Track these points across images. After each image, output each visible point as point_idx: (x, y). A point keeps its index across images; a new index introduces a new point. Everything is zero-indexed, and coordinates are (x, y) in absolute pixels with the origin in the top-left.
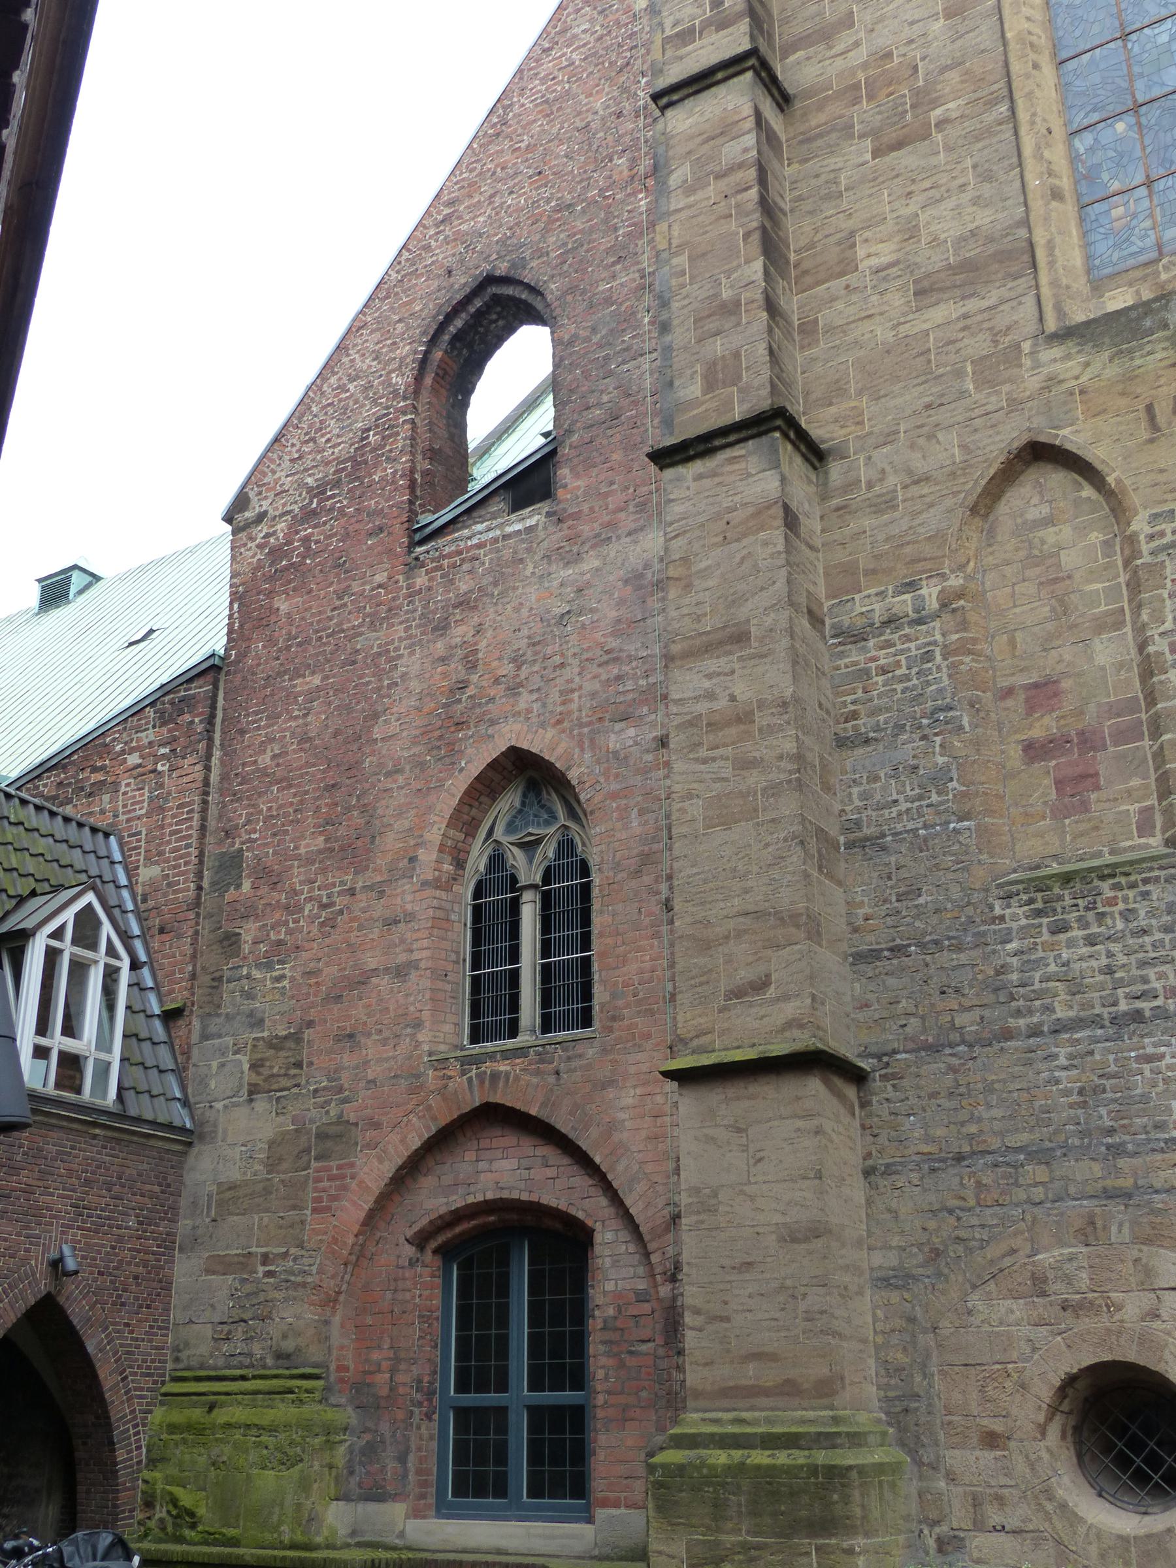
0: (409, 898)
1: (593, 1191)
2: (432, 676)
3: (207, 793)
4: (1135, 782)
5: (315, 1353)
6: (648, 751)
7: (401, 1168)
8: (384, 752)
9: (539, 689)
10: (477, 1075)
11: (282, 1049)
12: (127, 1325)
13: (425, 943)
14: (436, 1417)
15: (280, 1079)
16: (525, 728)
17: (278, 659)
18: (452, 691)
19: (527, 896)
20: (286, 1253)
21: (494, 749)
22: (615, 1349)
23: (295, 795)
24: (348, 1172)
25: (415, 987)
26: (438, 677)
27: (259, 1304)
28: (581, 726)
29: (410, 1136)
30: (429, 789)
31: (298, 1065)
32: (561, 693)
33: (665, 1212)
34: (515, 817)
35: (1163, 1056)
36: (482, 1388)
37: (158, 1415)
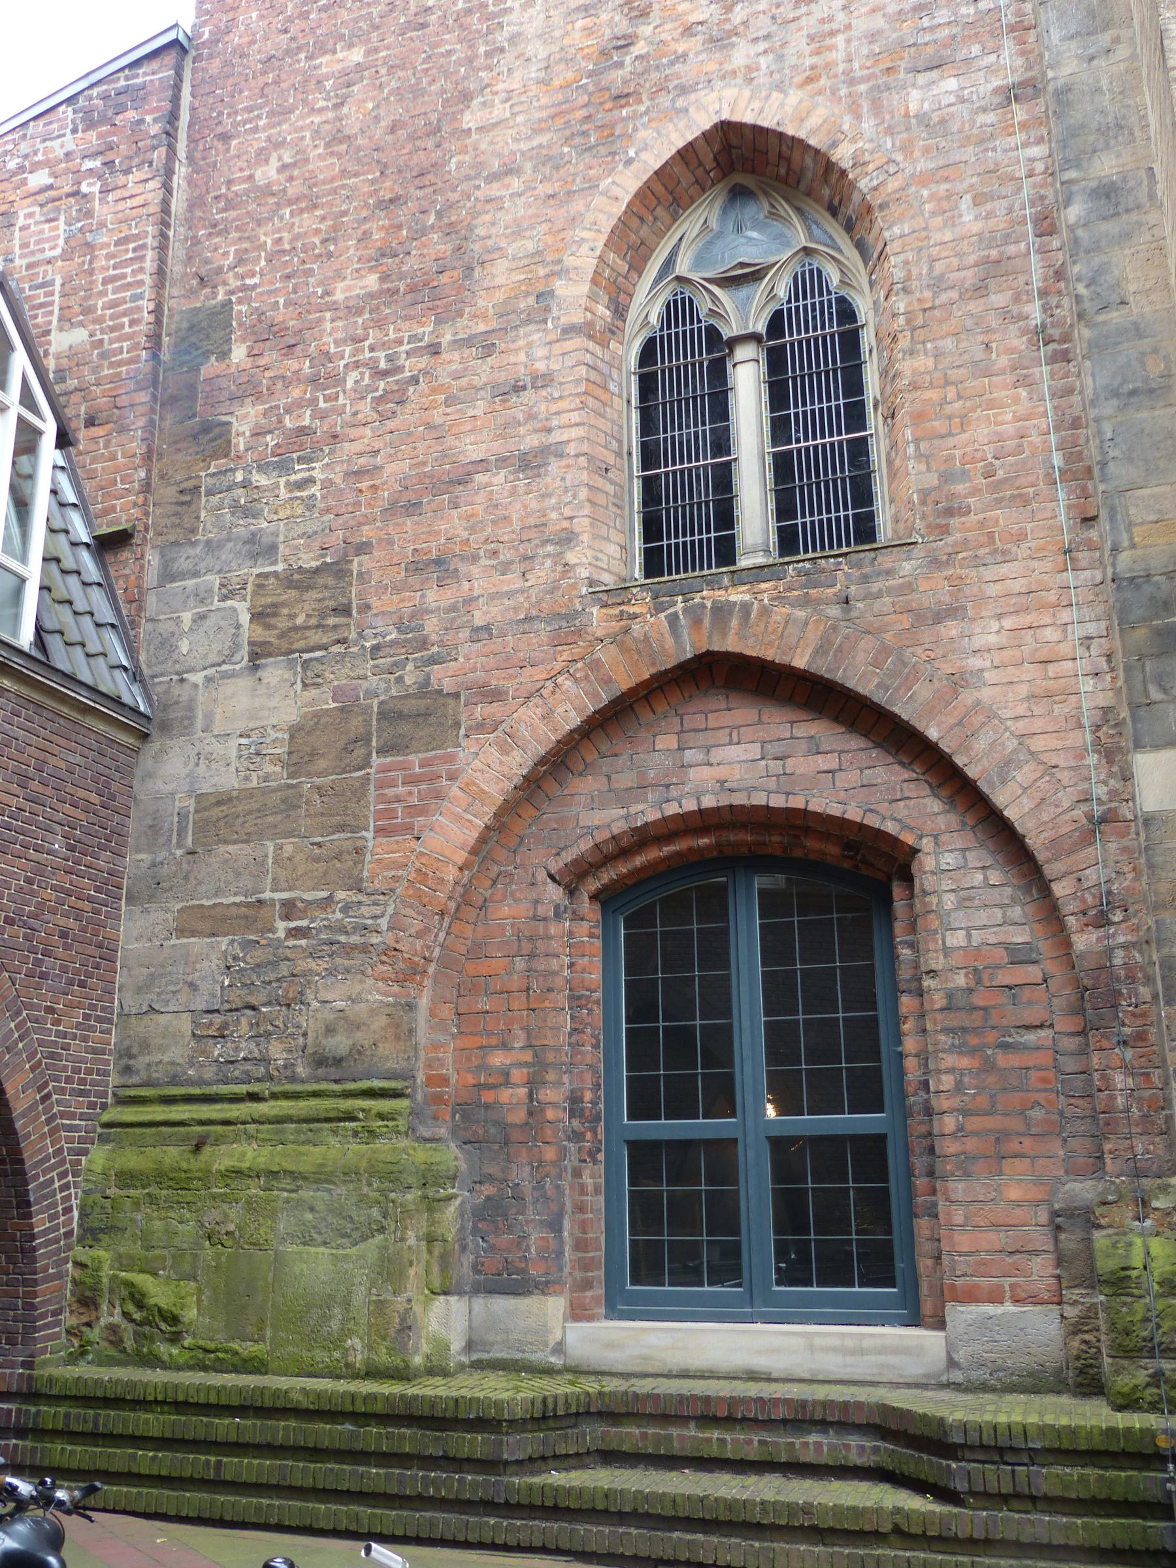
0: (541, 352)
1: (911, 789)
2: (567, 33)
3: (165, 224)
5: (389, 1055)
6: (985, 110)
7: (542, 761)
8: (483, 146)
9: (767, 37)
10: (685, 610)
11: (309, 587)
12: (50, 1010)
13: (575, 417)
14: (601, 1156)
15: (308, 633)
16: (747, 93)
17: (286, 31)
18: (604, 53)
19: (744, 352)
20: (329, 900)
21: (689, 127)
22: (974, 1041)
23: (323, 218)
24: (443, 769)
25: (558, 483)
26: (577, 35)
27: (278, 980)
28: (852, 82)
29: (560, 710)
30: (569, 193)
31: (345, 611)
32: (811, 38)
33: (1078, 813)
34: (710, 243)
36: (681, 1108)
37: (98, 1157)
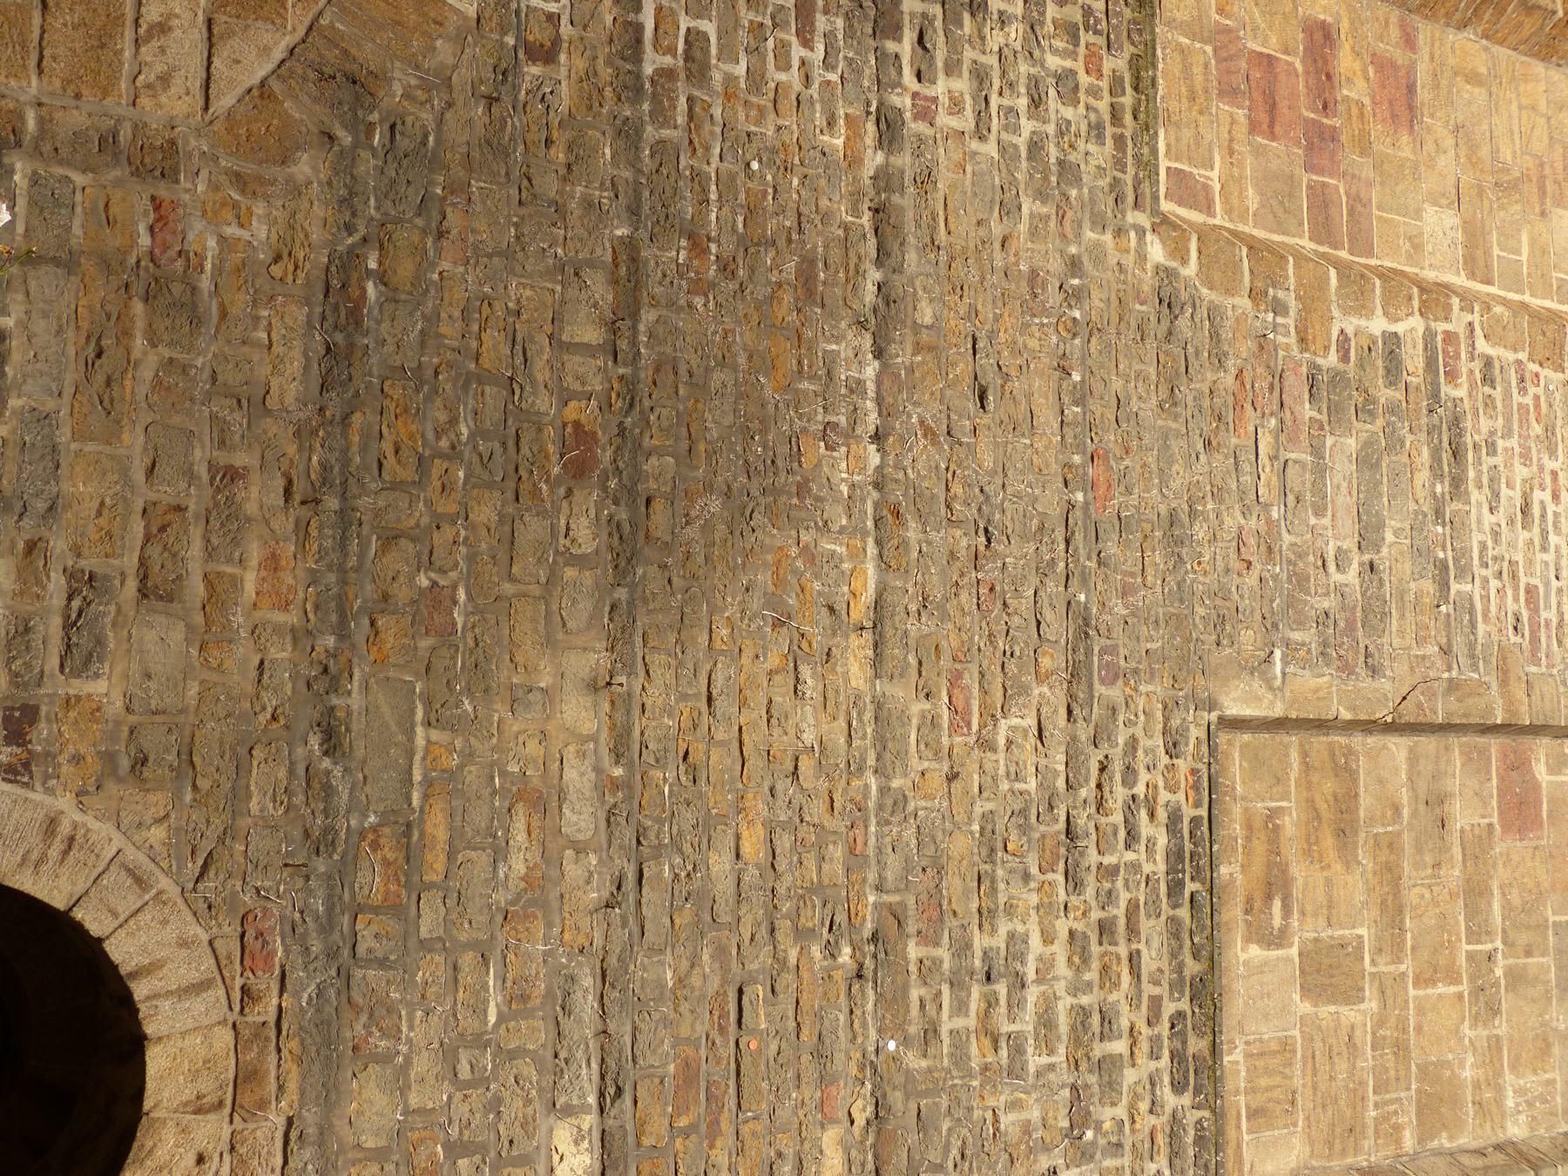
4: (1252, 200)
35: (807, 44)
